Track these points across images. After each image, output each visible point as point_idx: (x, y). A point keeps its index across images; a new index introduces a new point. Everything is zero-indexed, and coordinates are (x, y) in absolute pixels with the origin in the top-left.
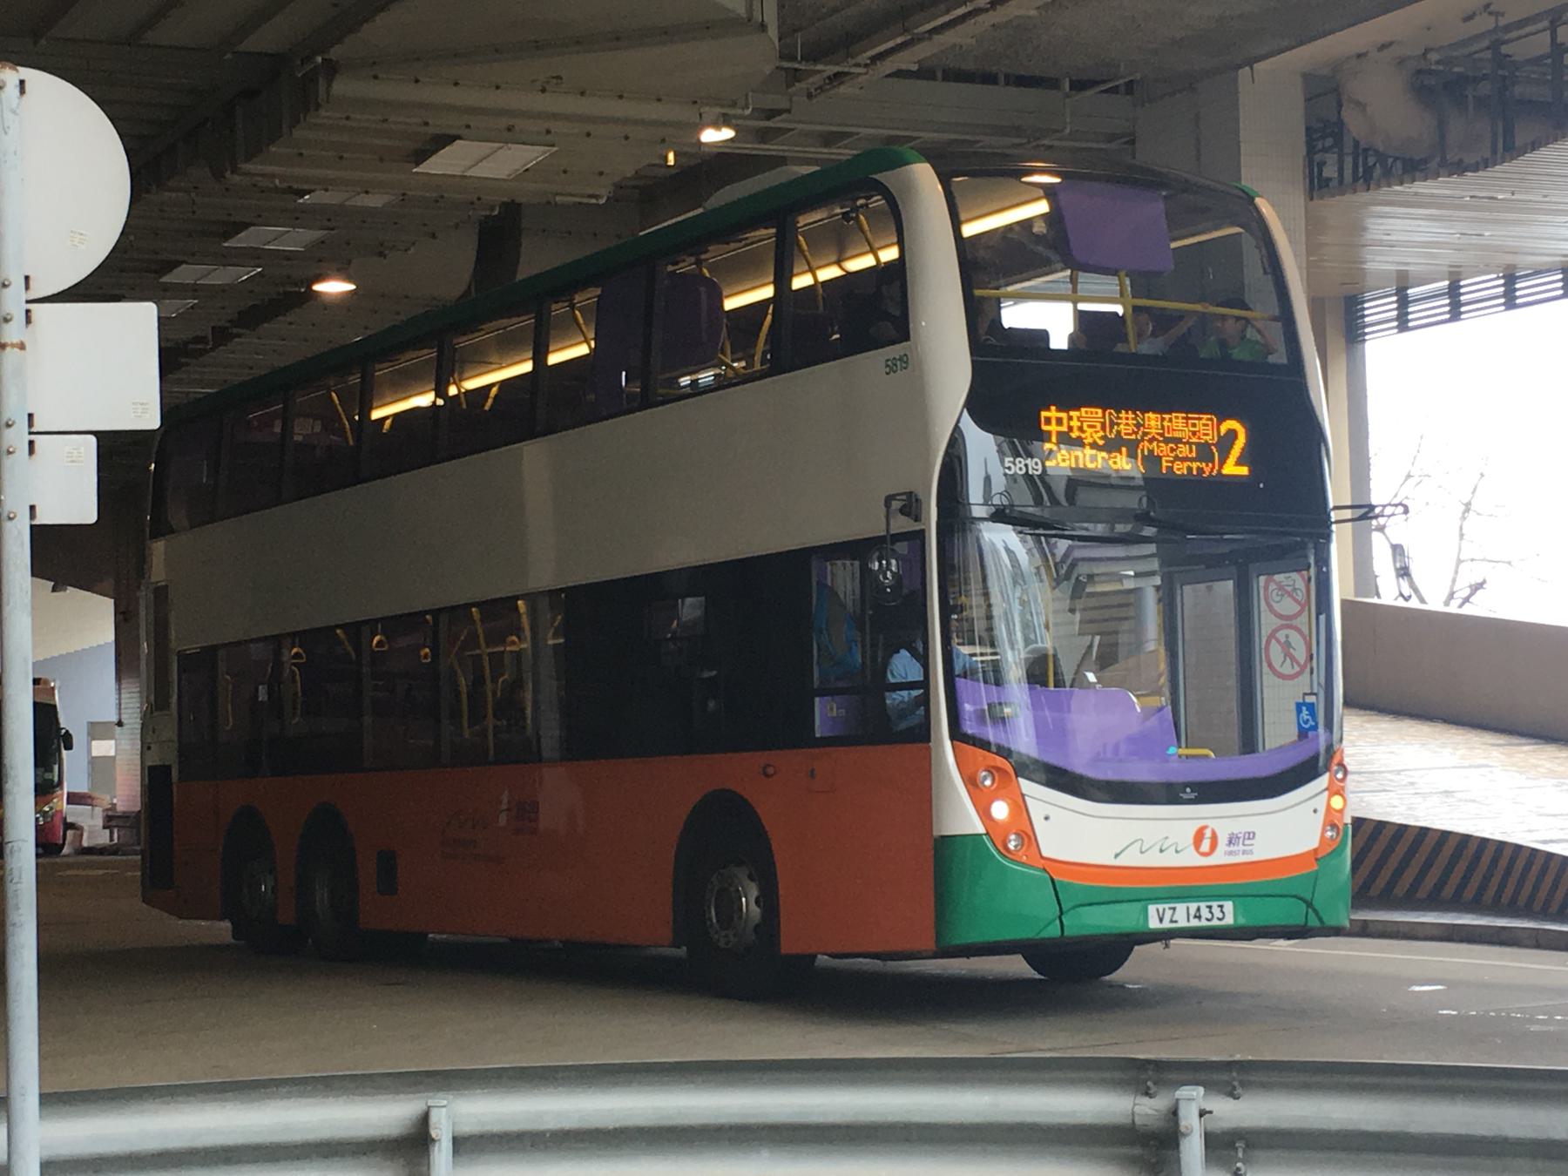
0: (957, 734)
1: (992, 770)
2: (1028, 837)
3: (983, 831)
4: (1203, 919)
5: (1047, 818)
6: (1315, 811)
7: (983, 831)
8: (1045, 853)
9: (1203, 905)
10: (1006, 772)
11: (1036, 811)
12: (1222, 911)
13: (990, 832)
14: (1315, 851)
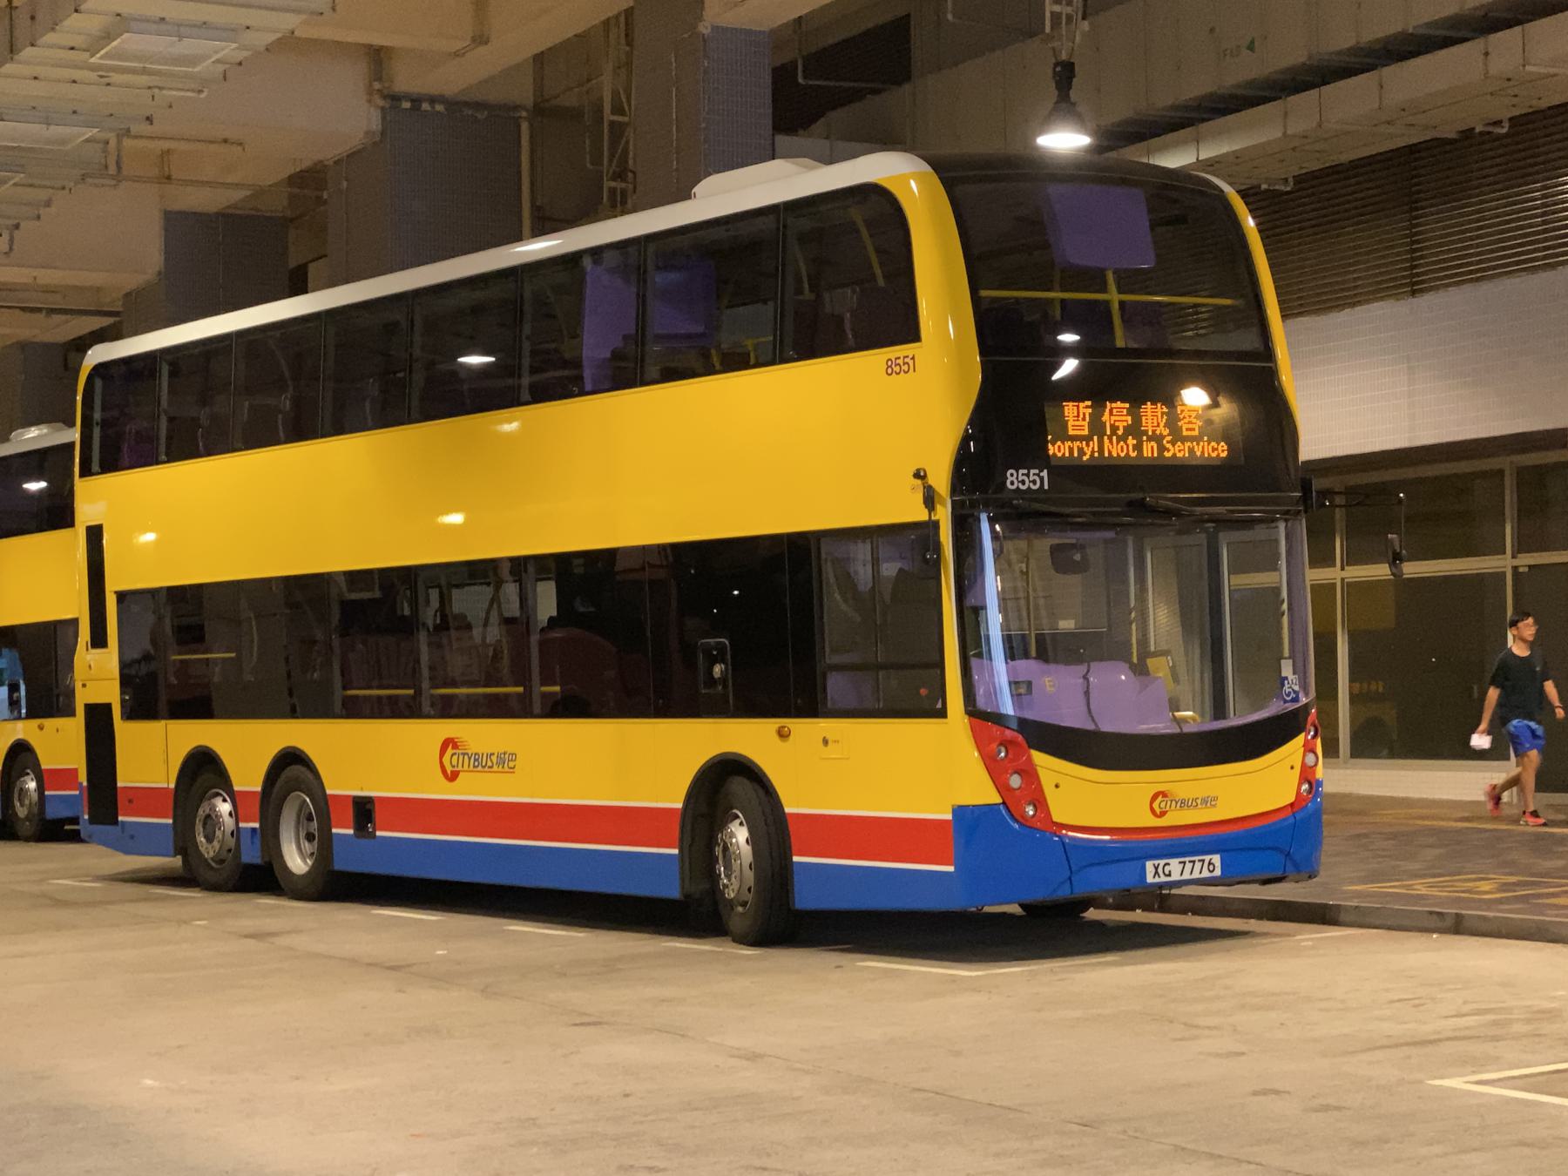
0: (972, 710)
2: (1040, 802)
3: (998, 800)
5: (1057, 786)
6: (1292, 768)
7: (998, 800)
8: (1057, 817)
10: (1019, 745)
11: (1047, 780)
13: (1007, 802)
14: (1292, 805)
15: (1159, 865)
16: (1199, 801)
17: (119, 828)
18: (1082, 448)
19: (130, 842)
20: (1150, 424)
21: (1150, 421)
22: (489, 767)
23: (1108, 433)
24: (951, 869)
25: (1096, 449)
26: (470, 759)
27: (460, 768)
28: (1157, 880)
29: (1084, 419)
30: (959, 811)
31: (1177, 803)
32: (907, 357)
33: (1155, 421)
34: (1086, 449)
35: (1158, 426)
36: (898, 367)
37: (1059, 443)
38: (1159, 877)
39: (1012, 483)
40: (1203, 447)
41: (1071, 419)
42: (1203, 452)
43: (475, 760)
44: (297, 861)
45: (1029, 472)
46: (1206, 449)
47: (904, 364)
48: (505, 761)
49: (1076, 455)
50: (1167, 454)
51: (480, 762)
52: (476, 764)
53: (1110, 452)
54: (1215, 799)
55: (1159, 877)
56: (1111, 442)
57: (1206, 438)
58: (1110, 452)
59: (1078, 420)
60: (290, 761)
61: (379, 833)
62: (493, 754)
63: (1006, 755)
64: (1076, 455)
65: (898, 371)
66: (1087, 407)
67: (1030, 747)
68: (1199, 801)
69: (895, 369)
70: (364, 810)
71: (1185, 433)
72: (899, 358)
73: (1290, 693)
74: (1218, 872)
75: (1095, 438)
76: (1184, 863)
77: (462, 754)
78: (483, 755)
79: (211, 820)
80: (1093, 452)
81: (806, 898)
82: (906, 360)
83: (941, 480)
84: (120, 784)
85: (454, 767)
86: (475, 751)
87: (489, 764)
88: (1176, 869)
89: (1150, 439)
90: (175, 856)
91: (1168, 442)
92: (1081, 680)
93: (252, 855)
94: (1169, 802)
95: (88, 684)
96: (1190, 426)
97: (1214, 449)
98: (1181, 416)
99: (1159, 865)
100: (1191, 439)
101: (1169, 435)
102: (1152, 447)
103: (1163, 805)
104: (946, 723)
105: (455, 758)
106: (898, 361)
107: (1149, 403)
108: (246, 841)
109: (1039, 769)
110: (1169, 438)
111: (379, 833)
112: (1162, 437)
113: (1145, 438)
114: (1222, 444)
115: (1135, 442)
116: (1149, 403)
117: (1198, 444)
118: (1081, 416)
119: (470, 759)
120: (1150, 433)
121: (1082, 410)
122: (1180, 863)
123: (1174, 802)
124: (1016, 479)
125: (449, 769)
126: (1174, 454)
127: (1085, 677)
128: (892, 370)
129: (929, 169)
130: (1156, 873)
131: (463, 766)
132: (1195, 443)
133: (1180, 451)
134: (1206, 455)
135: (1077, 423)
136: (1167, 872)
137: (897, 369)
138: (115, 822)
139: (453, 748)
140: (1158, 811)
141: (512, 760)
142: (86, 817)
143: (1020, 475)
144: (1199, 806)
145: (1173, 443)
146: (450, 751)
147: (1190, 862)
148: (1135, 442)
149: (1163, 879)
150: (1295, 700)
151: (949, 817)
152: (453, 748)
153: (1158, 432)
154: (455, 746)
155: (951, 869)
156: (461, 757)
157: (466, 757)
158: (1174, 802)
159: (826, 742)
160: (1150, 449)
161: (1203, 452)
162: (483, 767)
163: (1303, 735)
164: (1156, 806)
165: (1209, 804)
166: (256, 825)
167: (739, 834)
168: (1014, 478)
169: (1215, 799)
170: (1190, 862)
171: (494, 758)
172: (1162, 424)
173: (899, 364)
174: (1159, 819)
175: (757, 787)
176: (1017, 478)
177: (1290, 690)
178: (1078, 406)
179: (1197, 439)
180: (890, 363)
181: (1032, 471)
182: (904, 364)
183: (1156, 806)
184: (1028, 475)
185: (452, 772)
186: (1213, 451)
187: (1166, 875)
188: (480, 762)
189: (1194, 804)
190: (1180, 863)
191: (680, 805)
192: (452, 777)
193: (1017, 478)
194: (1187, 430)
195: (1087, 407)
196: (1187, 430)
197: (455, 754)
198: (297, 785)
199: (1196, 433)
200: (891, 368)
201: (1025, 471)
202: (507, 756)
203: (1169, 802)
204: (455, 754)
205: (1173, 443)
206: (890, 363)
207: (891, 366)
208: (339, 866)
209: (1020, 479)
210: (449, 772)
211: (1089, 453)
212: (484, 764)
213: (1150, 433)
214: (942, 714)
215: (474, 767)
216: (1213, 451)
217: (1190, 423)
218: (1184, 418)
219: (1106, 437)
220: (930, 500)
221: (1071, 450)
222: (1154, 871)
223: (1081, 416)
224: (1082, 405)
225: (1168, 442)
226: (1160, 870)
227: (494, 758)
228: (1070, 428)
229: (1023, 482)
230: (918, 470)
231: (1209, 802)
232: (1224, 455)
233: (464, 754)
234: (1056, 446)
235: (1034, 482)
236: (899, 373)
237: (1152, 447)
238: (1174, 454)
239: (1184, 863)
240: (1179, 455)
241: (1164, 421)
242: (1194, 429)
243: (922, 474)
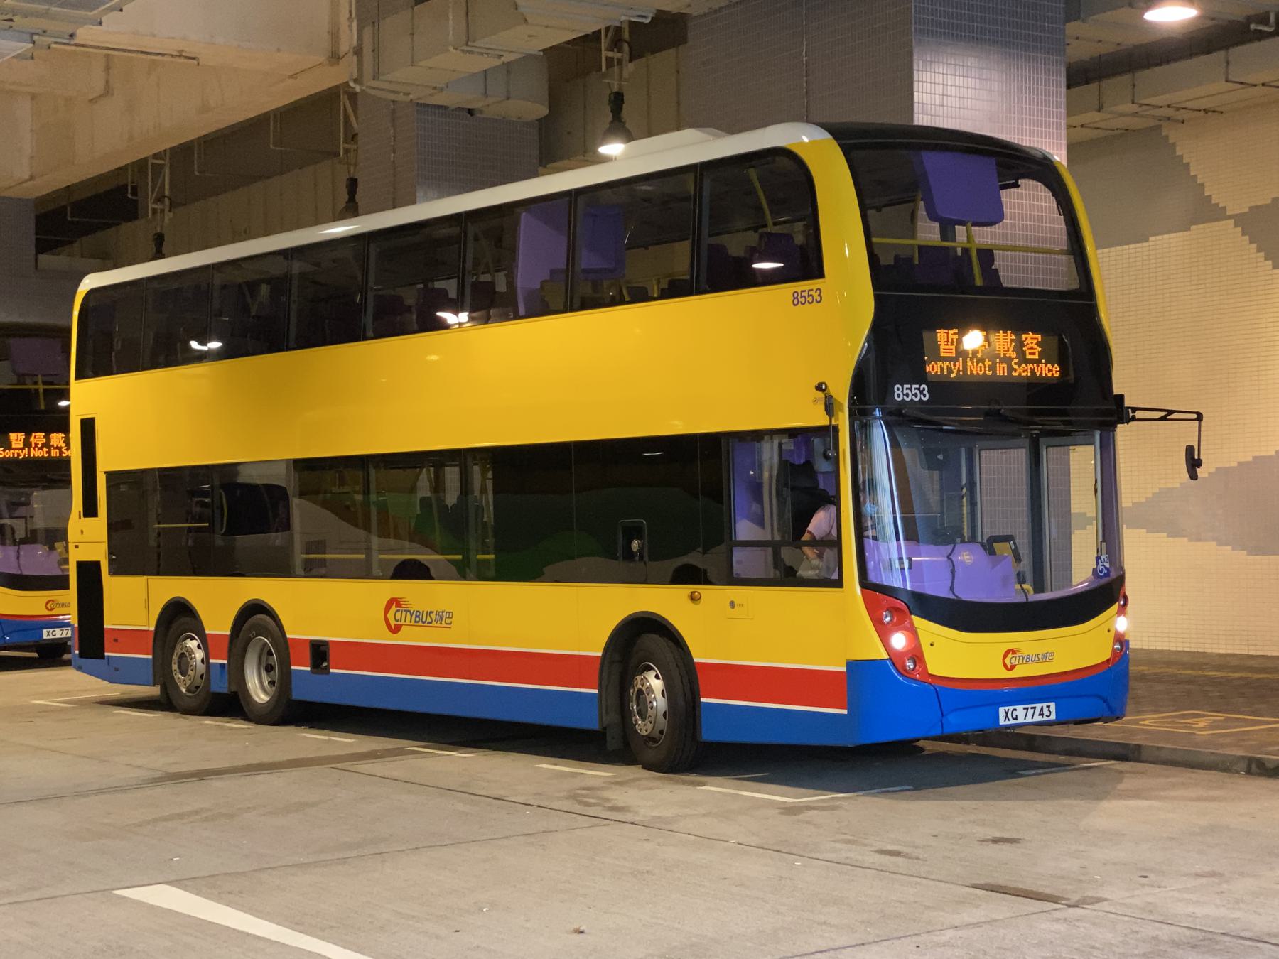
0: (865, 583)
1: (893, 610)
3: (886, 656)
4: (1044, 716)
5: (932, 645)
7: (886, 656)
8: (931, 671)
9: (1045, 705)
12: (1049, 710)
13: (892, 657)
15: (1008, 710)
16: (1040, 656)
17: (104, 662)
18: (951, 367)
19: (115, 674)
20: (1002, 349)
21: (1002, 346)
23: (970, 355)
24: (845, 712)
25: (961, 369)
27: (403, 622)
28: (1007, 722)
29: (952, 344)
30: (850, 664)
31: (1023, 659)
32: (812, 290)
33: (1006, 346)
34: (953, 368)
35: (1008, 351)
36: (803, 298)
37: (933, 363)
38: (1009, 720)
39: (899, 396)
40: (1041, 368)
41: (943, 343)
42: (1041, 373)
43: (416, 616)
44: (258, 690)
45: (911, 387)
46: (1043, 371)
47: (809, 296)
48: (441, 618)
49: (946, 373)
50: (1014, 374)
51: (420, 619)
52: (417, 619)
53: (971, 371)
54: (1052, 654)
55: (1009, 720)
56: (972, 363)
57: (1043, 361)
58: (971, 371)
59: (947, 345)
60: (254, 611)
61: (331, 671)
62: (432, 612)
63: (891, 620)
64: (946, 373)
65: (803, 302)
66: (955, 334)
67: (911, 613)
68: (1040, 656)
69: (800, 300)
70: (319, 652)
71: (1028, 357)
72: (805, 291)
74: (1053, 717)
75: (961, 359)
76: (1027, 709)
77: (405, 611)
78: (423, 612)
79: (184, 658)
80: (959, 371)
81: (709, 733)
82: (810, 293)
83: (842, 392)
84: (106, 626)
85: (397, 621)
86: (416, 609)
87: (429, 620)
88: (1021, 715)
89: (1001, 362)
90: (154, 685)
91: (1015, 364)
92: (946, 559)
93: (220, 686)
94: (1018, 658)
95: (80, 545)
96: (1032, 351)
97: (1050, 370)
98: (1025, 343)
99: (1008, 710)
100: (1033, 361)
101: (1016, 358)
102: (1003, 368)
103: (1013, 661)
104: (843, 592)
105: (398, 614)
106: (803, 294)
107: (1001, 332)
108: (215, 673)
109: (918, 630)
110: (1016, 361)
111: (331, 671)
112: (1011, 359)
113: (998, 360)
114: (1056, 366)
115: (990, 363)
116: (1001, 332)
117: (1038, 366)
118: (950, 341)
120: (1002, 356)
121: (951, 337)
122: (1024, 709)
123: (1021, 658)
124: (905, 393)
125: (393, 623)
126: (1020, 374)
127: (948, 557)
128: (798, 301)
129: (830, 137)
130: (1007, 717)
131: (405, 621)
132: (1035, 365)
133: (1024, 371)
134: (1044, 375)
135: (947, 347)
136: (1014, 717)
137: (803, 300)
138: (103, 657)
140: (1009, 665)
141: (449, 618)
142: (77, 652)
143: (905, 389)
144: (1041, 661)
145: (1019, 364)
146: (394, 609)
147: (1032, 708)
148: (990, 363)
149: (1012, 722)
150: (1107, 575)
151: (844, 669)
153: (1008, 356)
154: (399, 605)
155: (845, 712)
156: (404, 613)
158: (1021, 658)
159: (732, 605)
160: (1002, 370)
161: (1041, 373)
163: (1117, 604)
164: (1007, 661)
165: (1048, 660)
166: (225, 662)
167: (654, 683)
168: (900, 392)
169: (1052, 654)
170: (1032, 708)
171: (433, 616)
172: (1011, 349)
173: (804, 296)
174: (1011, 672)
175: (671, 643)
176: (902, 391)
178: (948, 333)
179: (1038, 362)
180: (796, 295)
181: (914, 386)
182: (809, 296)
183: (1007, 661)
184: (910, 389)
185: (395, 625)
186: (1049, 372)
187: (1014, 719)
188: (420, 619)
189: (1037, 659)
190: (1024, 709)
191: (600, 654)
192: (395, 629)
193: (902, 391)
194: (1030, 354)
195: (955, 334)
196: (1030, 354)
197: (399, 611)
198: (263, 631)
199: (1036, 357)
200: (797, 300)
201: (909, 386)
202: (444, 614)
203: (1018, 658)
205: (1019, 364)
206: (796, 295)
207: (797, 298)
208: (297, 695)
209: (905, 392)
210: (393, 626)
211: (955, 371)
213: (1002, 356)
214: (838, 583)
215: (415, 622)
216: (1049, 372)
217: (1032, 348)
218: (1028, 344)
219: (968, 359)
220: (830, 407)
221: (942, 369)
222: (1005, 715)
223: (950, 341)
224: (951, 332)
225: (1015, 364)
226: (1009, 715)
227: (433, 616)
228: (942, 351)
229: (907, 395)
230: (821, 384)
231: (1047, 657)
232: (1057, 375)
233: (406, 611)
234: (931, 366)
235: (916, 395)
236: (804, 304)
237: (1003, 368)
238: (1020, 374)
239: (1027, 709)
240: (1024, 374)
241: (1013, 346)
242: (1034, 354)
243: (824, 387)
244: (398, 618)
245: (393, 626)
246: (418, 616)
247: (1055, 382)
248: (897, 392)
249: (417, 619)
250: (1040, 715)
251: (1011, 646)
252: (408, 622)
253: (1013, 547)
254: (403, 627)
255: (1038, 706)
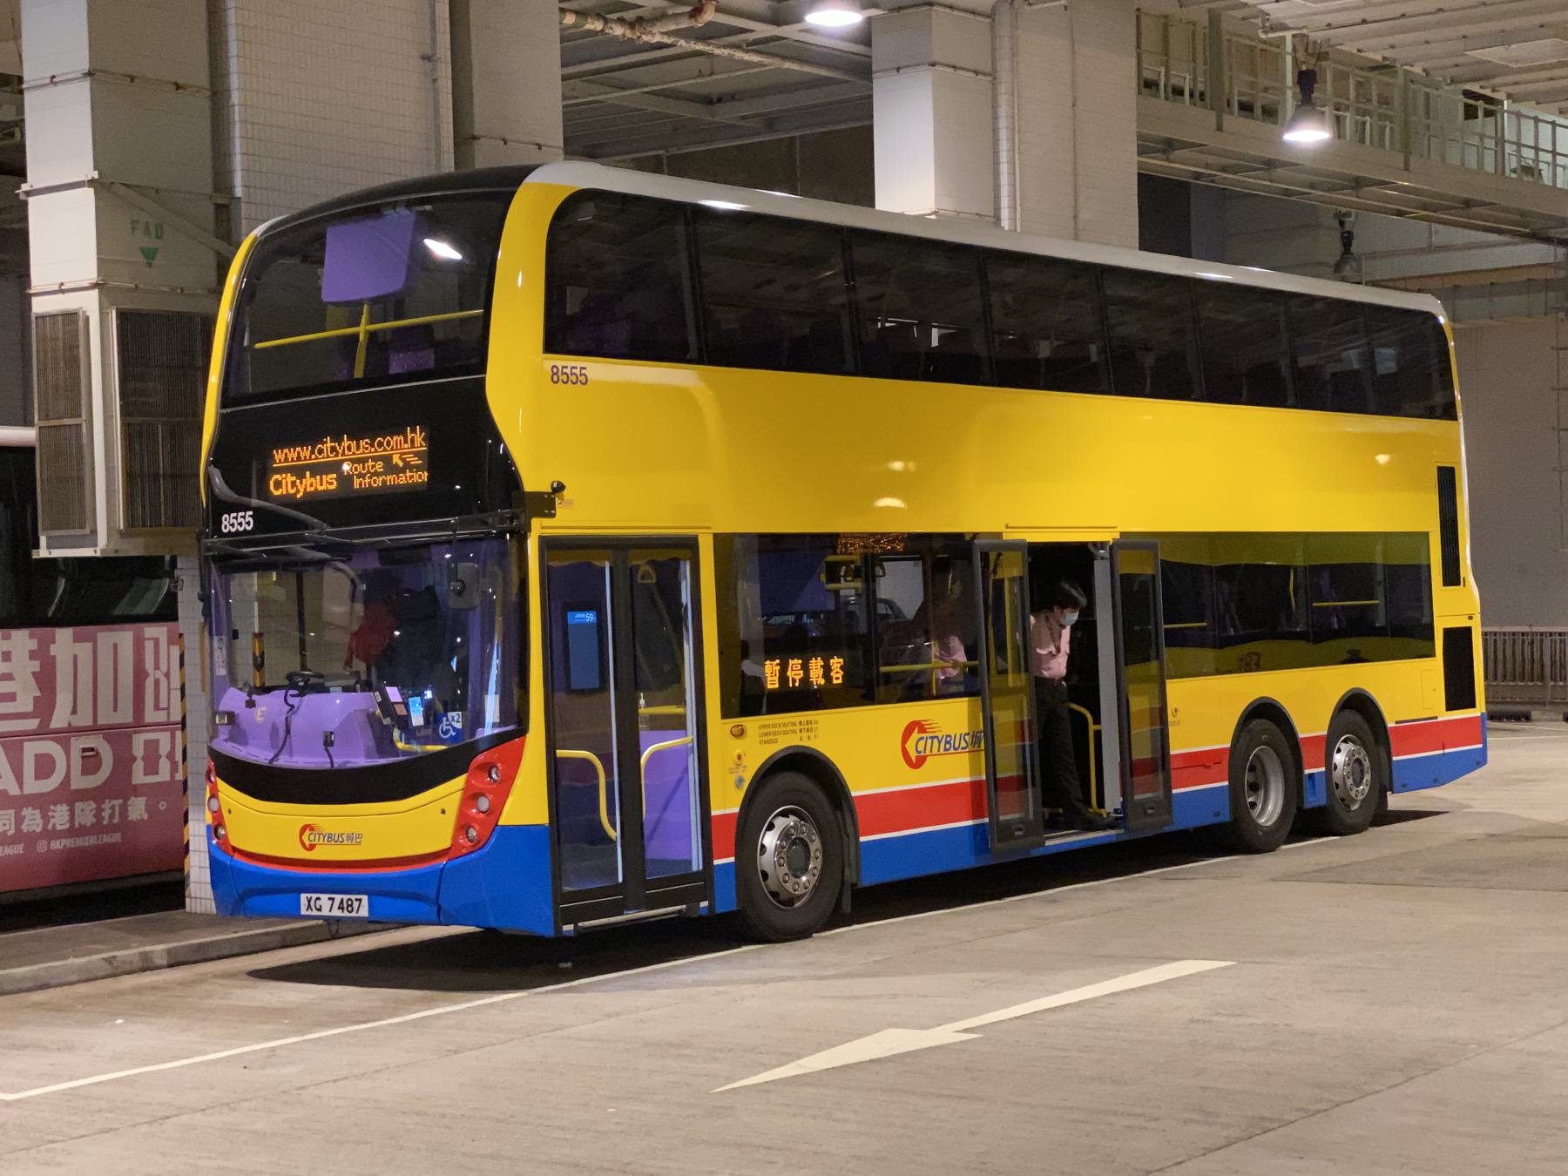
16: (345, 837)
22: (963, 748)
26: (940, 742)
28: (309, 913)
43: (947, 742)
68: (345, 837)
73: (448, 731)
77: (931, 738)
103: (312, 837)
119: (940, 742)
122: (330, 899)
130: (309, 906)
139: (919, 732)
140: (307, 843)
144: (345, 842)
146: (915, 735)
149: (315, 913)
152: (919, 732)
154: (922, 729)
156: (929, 741)
157: (935, 740)
162: (955, 749)
164: (305, 838)
169: (360, 836)
177: (449, 727)
184: (244, 517)
189: (340, 839)
190: (330, 899)
192: (917, 763)
197: (922, 738)
201: (235, 515)
204: (922, 738)
211: (302, 490)
212: (957, 746)
215: (945, 750)
222: (307, 903)
229: (233, 525)
231: (353, 838)
233: (932, 738)
239: (333, 899)
244: (921, 748)
245: (914, 760)
246: (949, 742)
247: (425, 488)
248: (224, 523)
249: (948, 746)
250: (339, 908)
251: (309, 820)
252: (935, 750)
253: (380, 699)
254: (928, 758)
255: (338, 897)
